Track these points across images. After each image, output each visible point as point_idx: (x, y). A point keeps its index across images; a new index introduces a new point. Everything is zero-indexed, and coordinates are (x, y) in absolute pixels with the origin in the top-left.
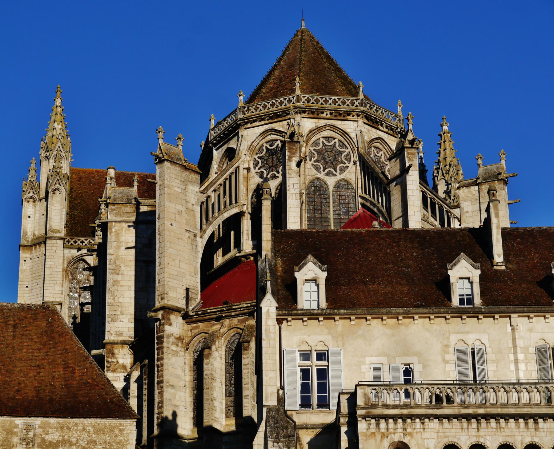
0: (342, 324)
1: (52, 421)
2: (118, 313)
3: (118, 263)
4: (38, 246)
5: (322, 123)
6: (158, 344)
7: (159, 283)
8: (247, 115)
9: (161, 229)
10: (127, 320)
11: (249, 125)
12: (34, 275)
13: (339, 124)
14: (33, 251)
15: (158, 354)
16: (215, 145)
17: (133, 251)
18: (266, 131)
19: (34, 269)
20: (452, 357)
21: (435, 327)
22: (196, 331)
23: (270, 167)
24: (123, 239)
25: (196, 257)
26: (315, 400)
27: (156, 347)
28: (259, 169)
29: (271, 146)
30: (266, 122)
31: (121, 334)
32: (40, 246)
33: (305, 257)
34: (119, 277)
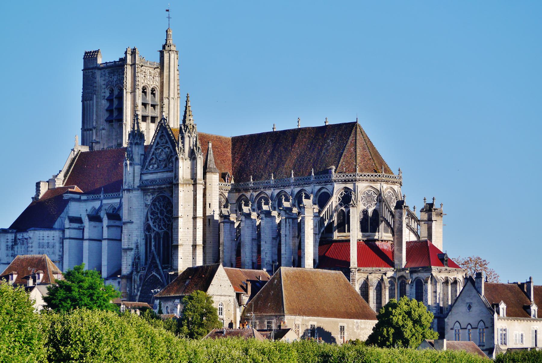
1: (363, 321)
2: (308, 256)
4: (188, 185)
6: (352, 281)
7: (352, 257)
9: (353, 235)
10: (311, 259)
11: (361, 182)
12: (186, 200)
13: (393, 186)
14: (185, 187)
16: (336, 182)
17: (313, 230)
18: (368, 186)
19: (186, 197)
20: (531, 332)
22: (361, 276)
23: (368, 202)
24: (309, 224)
25: (355, 243)
28: (363, 201)
29: (369, 192)
30: (368, 182)
33: (500, 301)
34: (308, 241)
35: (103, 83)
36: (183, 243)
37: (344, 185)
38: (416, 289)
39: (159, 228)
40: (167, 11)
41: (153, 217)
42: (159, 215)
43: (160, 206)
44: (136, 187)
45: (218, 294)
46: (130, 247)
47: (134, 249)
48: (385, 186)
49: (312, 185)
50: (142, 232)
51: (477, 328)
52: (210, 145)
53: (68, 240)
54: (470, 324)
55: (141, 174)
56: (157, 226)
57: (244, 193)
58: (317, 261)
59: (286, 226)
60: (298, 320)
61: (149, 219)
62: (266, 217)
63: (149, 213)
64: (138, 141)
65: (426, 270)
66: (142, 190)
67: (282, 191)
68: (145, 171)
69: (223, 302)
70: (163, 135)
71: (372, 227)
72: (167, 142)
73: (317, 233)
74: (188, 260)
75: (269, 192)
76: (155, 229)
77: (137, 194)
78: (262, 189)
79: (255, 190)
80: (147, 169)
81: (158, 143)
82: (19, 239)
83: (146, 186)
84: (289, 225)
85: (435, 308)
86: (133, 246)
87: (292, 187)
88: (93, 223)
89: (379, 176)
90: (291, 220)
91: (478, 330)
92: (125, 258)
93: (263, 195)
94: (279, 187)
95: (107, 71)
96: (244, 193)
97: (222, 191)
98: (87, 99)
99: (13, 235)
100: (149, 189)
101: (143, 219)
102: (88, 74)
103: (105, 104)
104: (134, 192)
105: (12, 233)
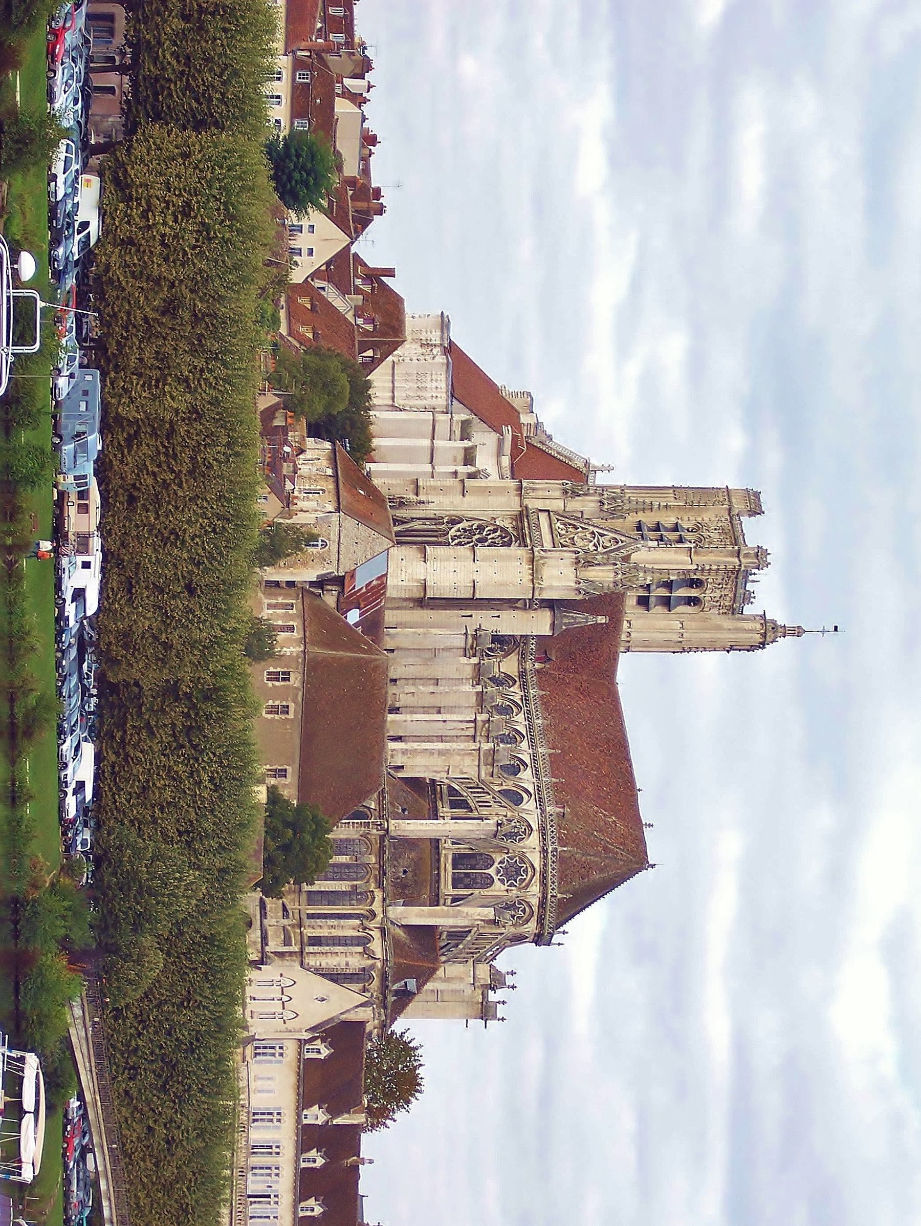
0: (295, 1064)
2: (409, 755)
3: (447, 755)
5: (535, 909)
8: (550, 855)
11: (542, 856)
15: (357, 823)
21: (293, 1105)
22: (373, 841)
24: (466, 757)
26: (258, 1051)
27: (363, 821)
31: (392, 756)
32: (530, 574)
34: (436, 755)
35: (706, 519)
36: (428, 563)
37: (535, 827)
38: (352, 937)
39: (455, 536)
40: (836, 629)
41: (474, 527)
42: (477, 536)
43: (493, 538)
44: (526, 502)
45: (342, 537)
46: (421, 491)
47: (418, 498)
48: (534, 902)
49: (534, 780)
50: (448, 513)
51: (284, 1008)
52: (601, 620)
53: (432, 418)
54: (291, 999)
55: (548, 511)
56: (459, 533)
57: (518, 683)
58: (400, 775)
59: (461, 721)
60: (296, 679)
61: (470, 523)
62: (477, 693)
63: (480, 522)
64: (606, 507)
65: (386, 950)
66: (521, 513)
67: (524, 737)
68: (554, 517)
69: (327, 547)
70: (618, 543)
71: (462, 875)
72: (604, 547)
73: (451, 776)
74: (400, 572)
75: (520, 718)
76: (453, 530)
77: (514, 505)
78: (526, 708)
79: (525, 698)
80: (558, 520)
81: (602, 535)
82: (432, 350)
83: (527, 516)
84: (463, 729)
85: (318, 964)
86: (422, 497)
87: (531, 751)
88: (461, 456)
89: (553, 889)
90: (471, 732)
91: (281, 1011)
92: (402, 482)
93: (515, 710)
94: (530, 732)
95: (726, 525)
96: (518, 683)
97: (522, 645)
98: (677, 494)
99: (438, 342)
100: (522, 521)
101: (470, 514)
102: (721, 494)
103: (669, 520)
104: (517, 499)
105: (442, 338)
